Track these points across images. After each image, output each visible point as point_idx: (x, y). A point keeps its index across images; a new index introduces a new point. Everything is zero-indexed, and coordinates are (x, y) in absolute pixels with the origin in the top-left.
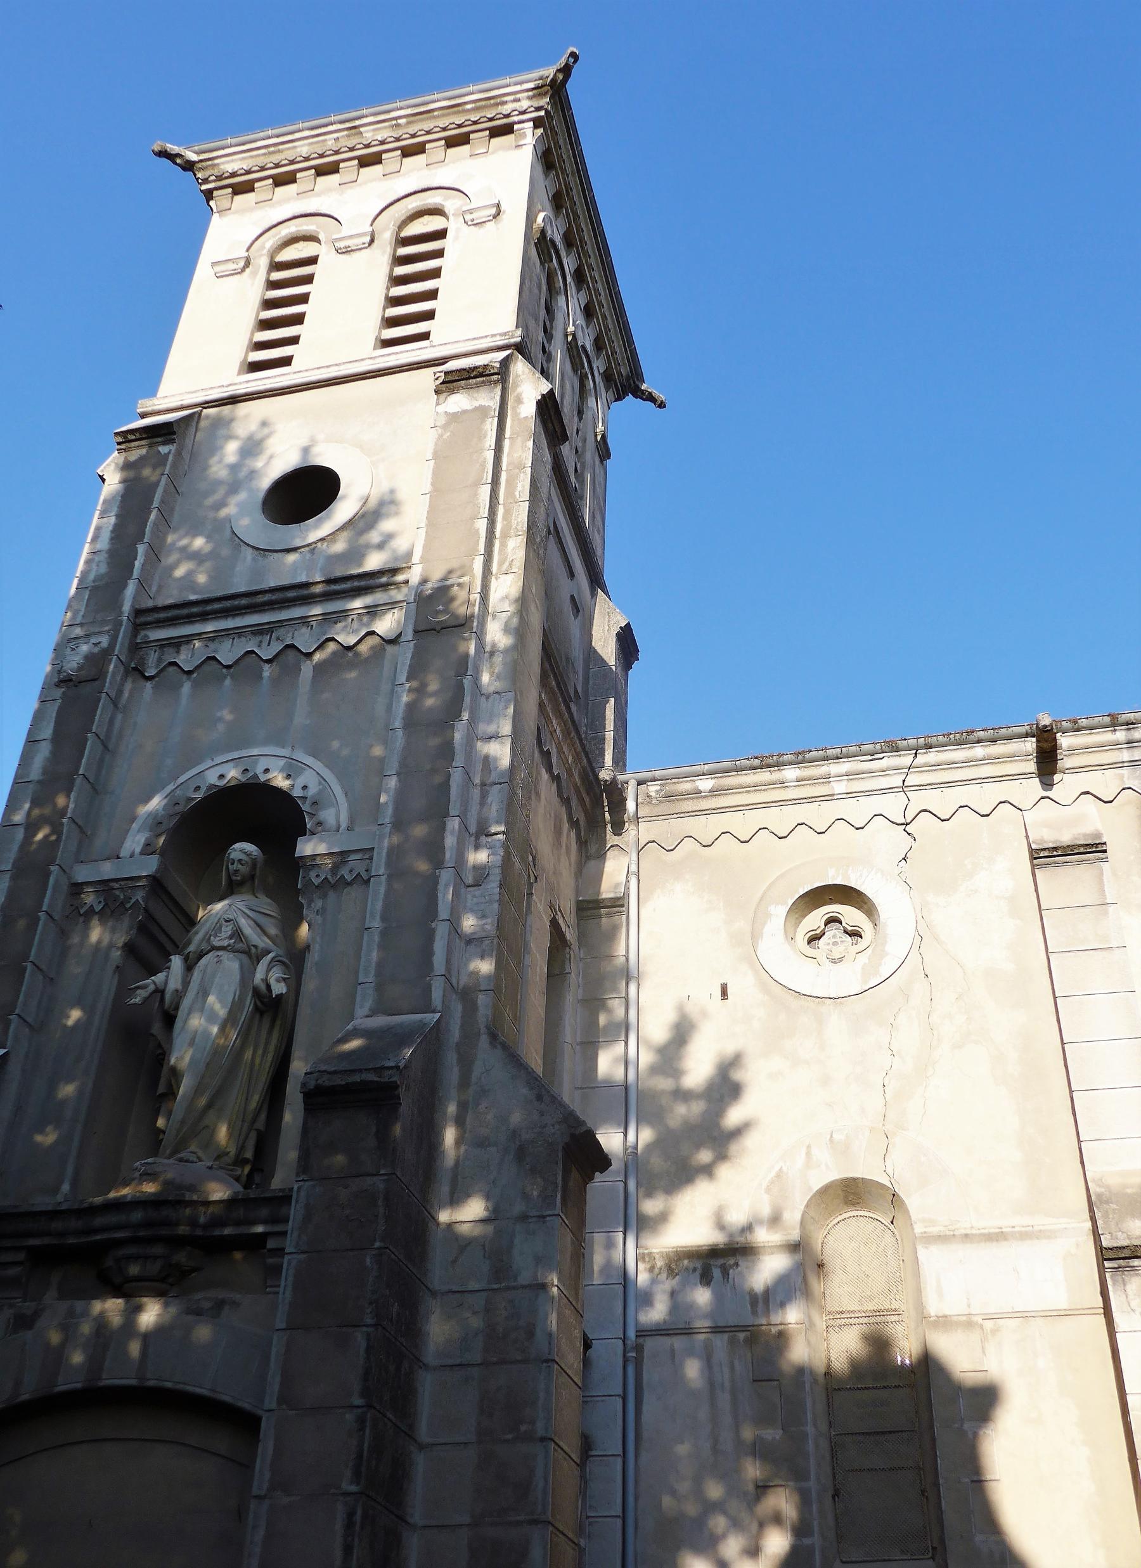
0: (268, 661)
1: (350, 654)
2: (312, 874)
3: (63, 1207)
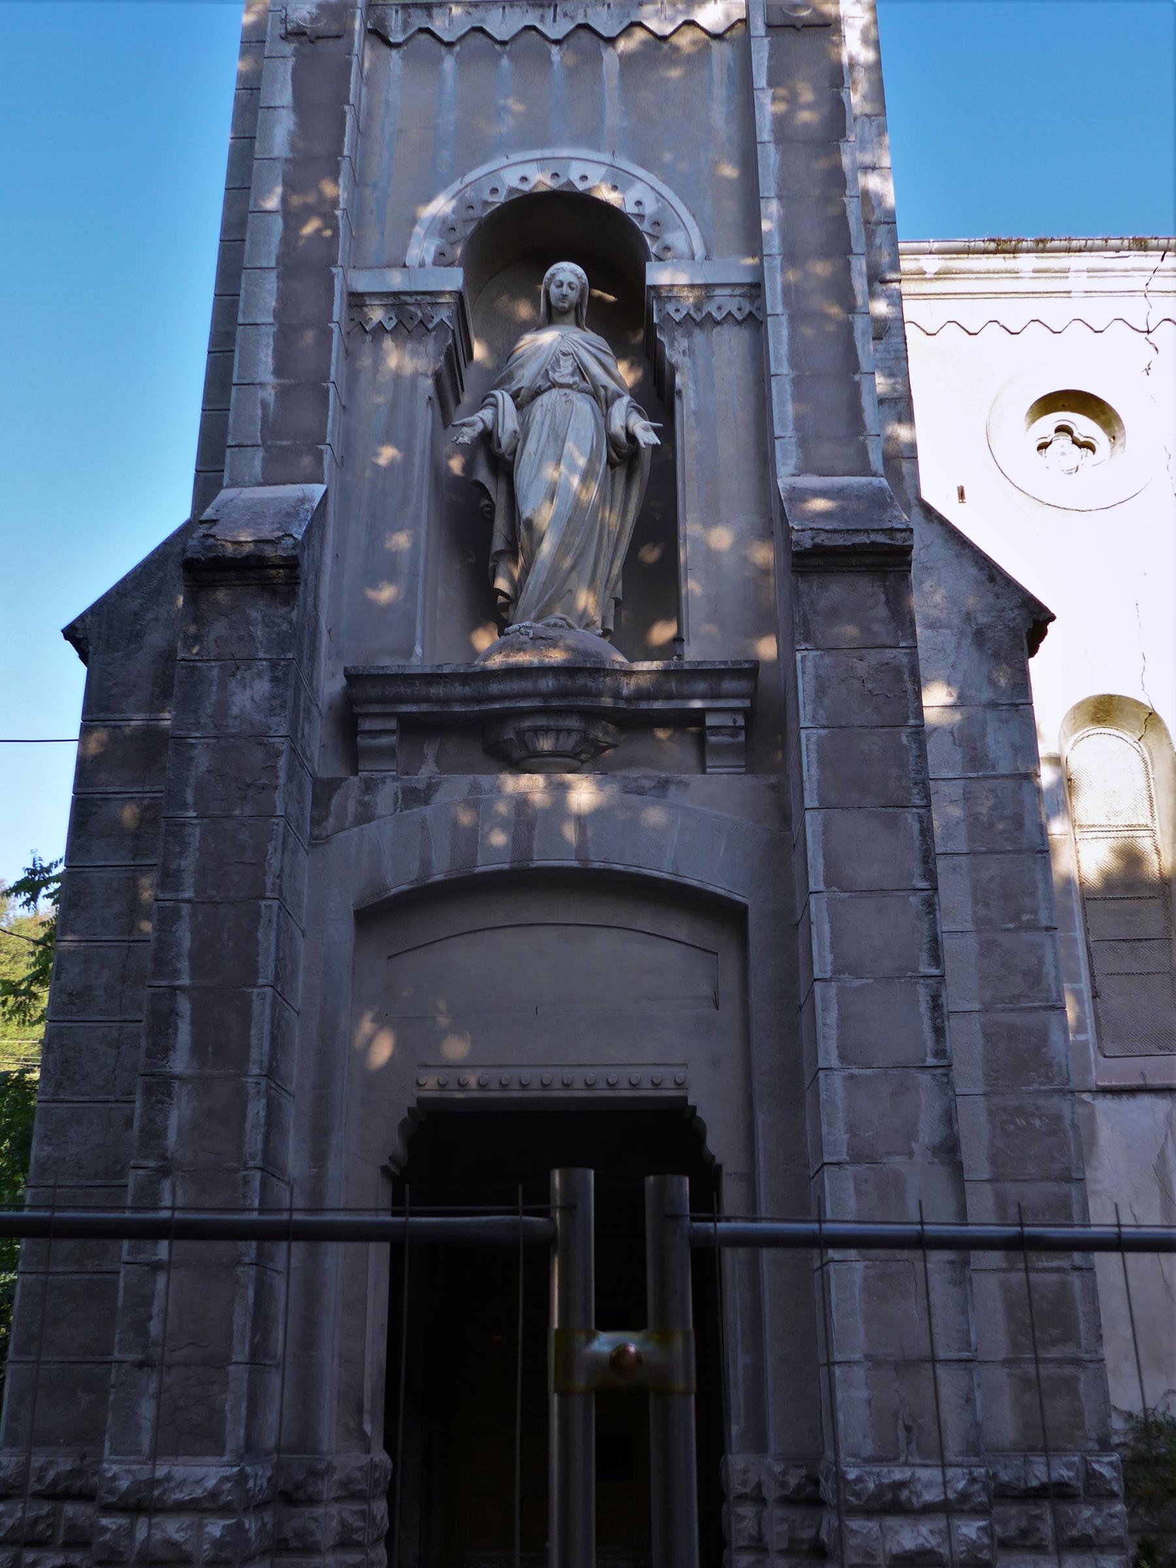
0: (557, 42)
1: (666, 46)
2: (670, 308)
3: (446, 670)
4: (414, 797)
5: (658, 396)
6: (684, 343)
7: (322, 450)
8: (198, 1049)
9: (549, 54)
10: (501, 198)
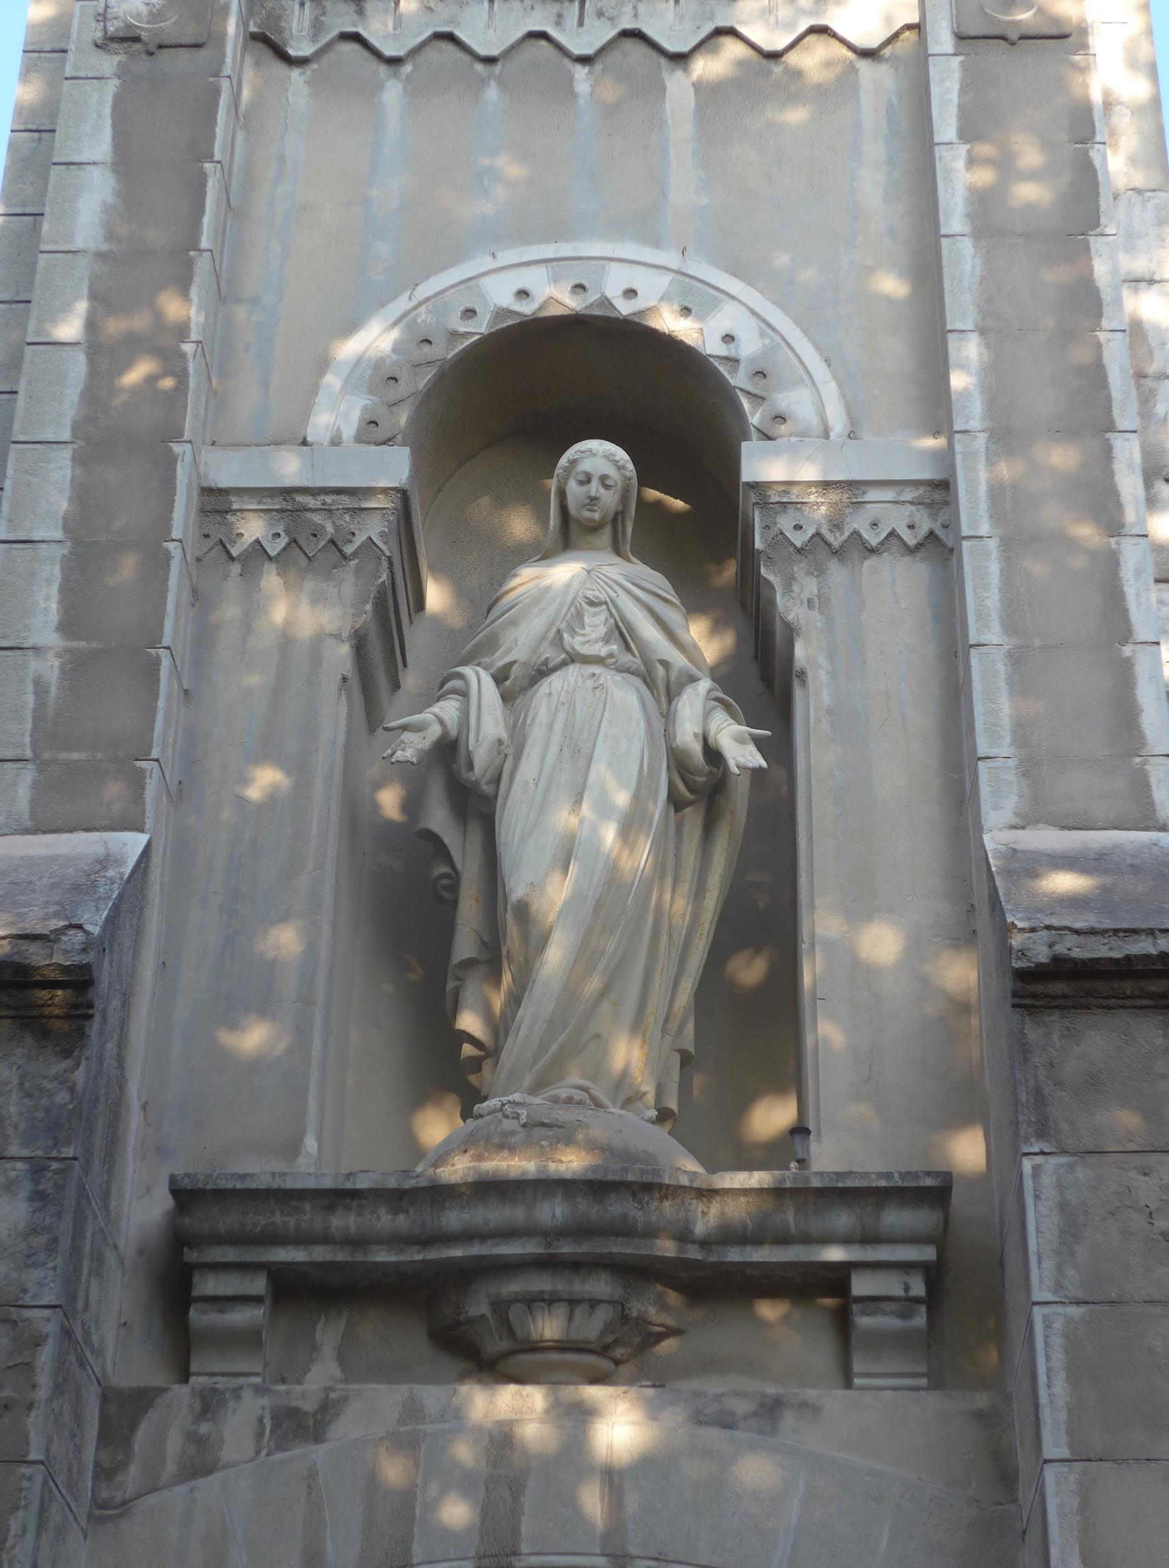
0: (584, 60)
1: (777, 69)
2: (785, 523)
3: (362, 1183)
4: (297, 1426)
5: (764, 679)
6: (809, 586)
7: (142, 771)
9: (570, 80)
10: (481, 326)
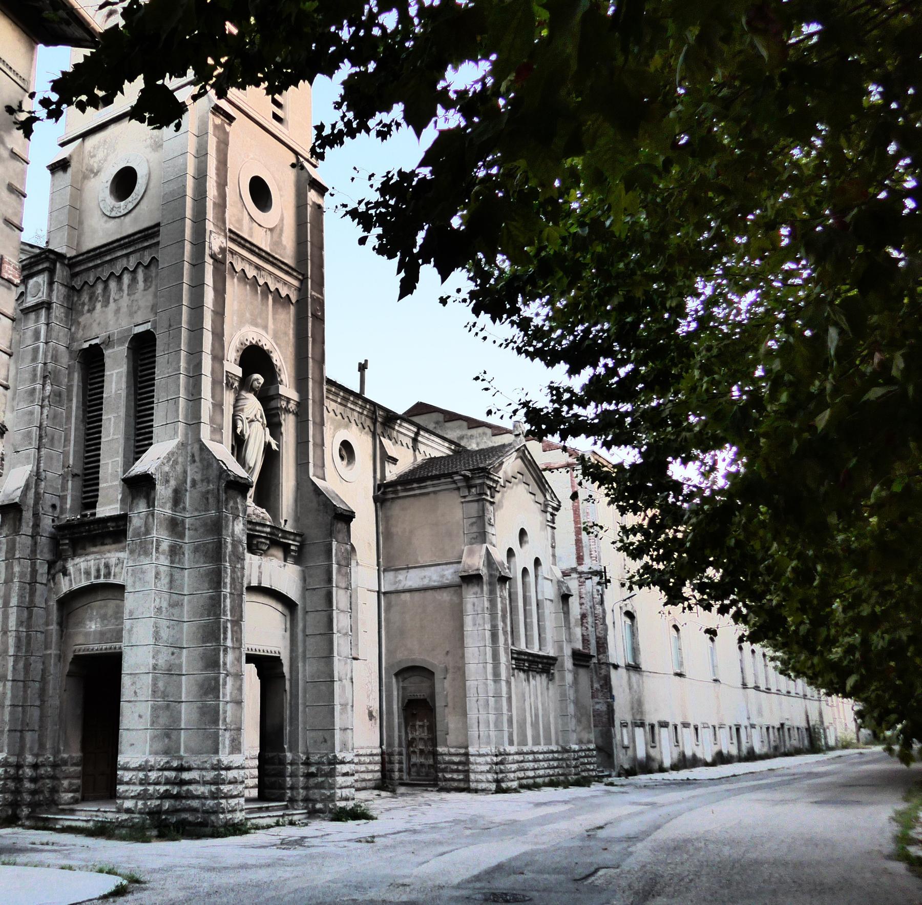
8: (232, 639)
